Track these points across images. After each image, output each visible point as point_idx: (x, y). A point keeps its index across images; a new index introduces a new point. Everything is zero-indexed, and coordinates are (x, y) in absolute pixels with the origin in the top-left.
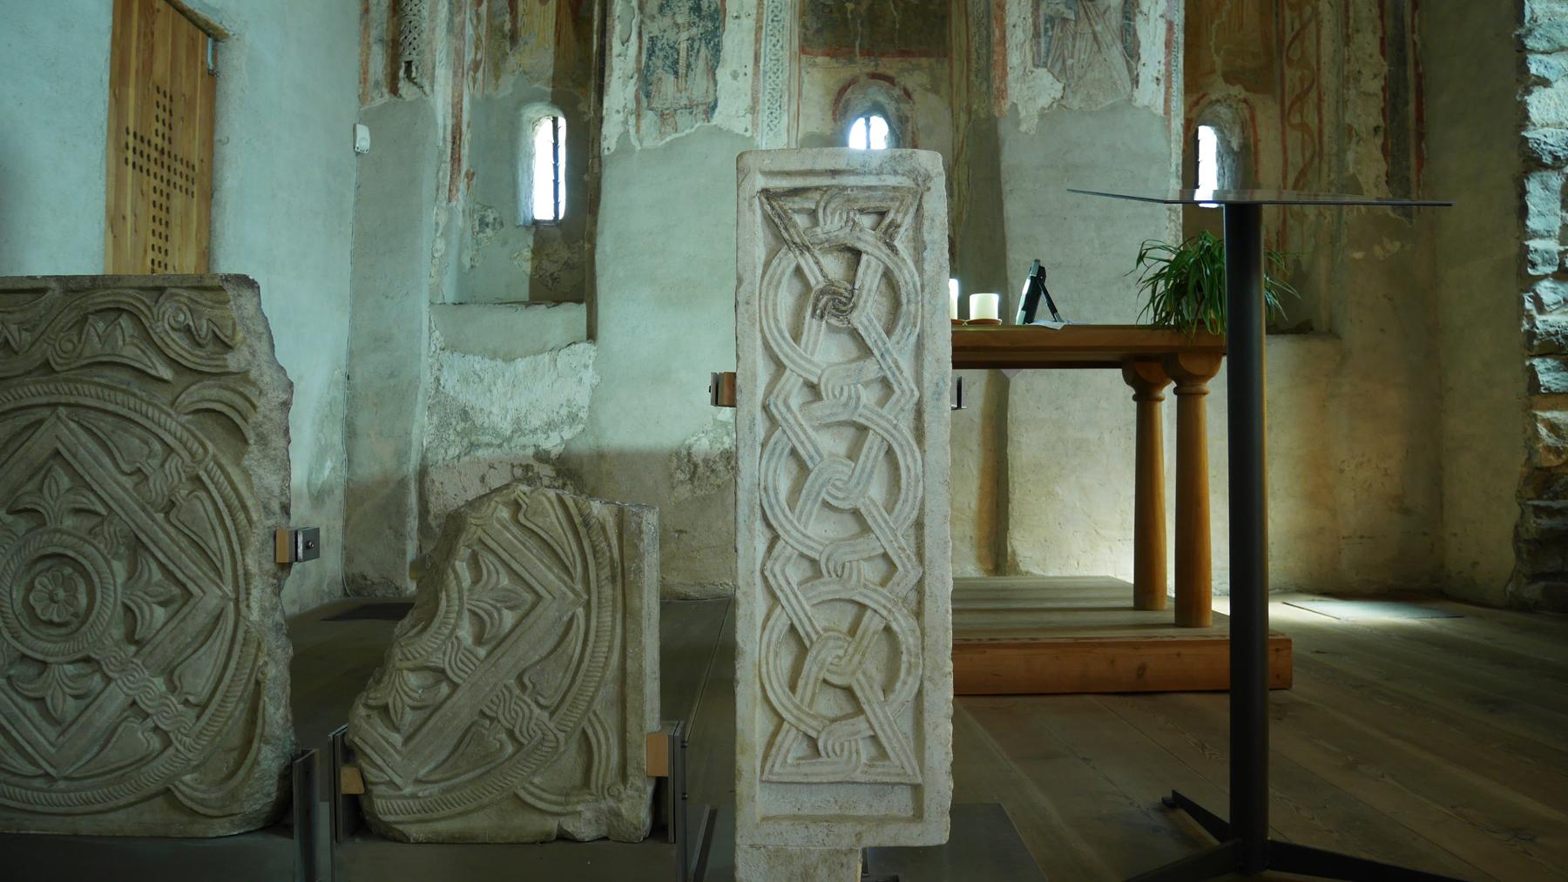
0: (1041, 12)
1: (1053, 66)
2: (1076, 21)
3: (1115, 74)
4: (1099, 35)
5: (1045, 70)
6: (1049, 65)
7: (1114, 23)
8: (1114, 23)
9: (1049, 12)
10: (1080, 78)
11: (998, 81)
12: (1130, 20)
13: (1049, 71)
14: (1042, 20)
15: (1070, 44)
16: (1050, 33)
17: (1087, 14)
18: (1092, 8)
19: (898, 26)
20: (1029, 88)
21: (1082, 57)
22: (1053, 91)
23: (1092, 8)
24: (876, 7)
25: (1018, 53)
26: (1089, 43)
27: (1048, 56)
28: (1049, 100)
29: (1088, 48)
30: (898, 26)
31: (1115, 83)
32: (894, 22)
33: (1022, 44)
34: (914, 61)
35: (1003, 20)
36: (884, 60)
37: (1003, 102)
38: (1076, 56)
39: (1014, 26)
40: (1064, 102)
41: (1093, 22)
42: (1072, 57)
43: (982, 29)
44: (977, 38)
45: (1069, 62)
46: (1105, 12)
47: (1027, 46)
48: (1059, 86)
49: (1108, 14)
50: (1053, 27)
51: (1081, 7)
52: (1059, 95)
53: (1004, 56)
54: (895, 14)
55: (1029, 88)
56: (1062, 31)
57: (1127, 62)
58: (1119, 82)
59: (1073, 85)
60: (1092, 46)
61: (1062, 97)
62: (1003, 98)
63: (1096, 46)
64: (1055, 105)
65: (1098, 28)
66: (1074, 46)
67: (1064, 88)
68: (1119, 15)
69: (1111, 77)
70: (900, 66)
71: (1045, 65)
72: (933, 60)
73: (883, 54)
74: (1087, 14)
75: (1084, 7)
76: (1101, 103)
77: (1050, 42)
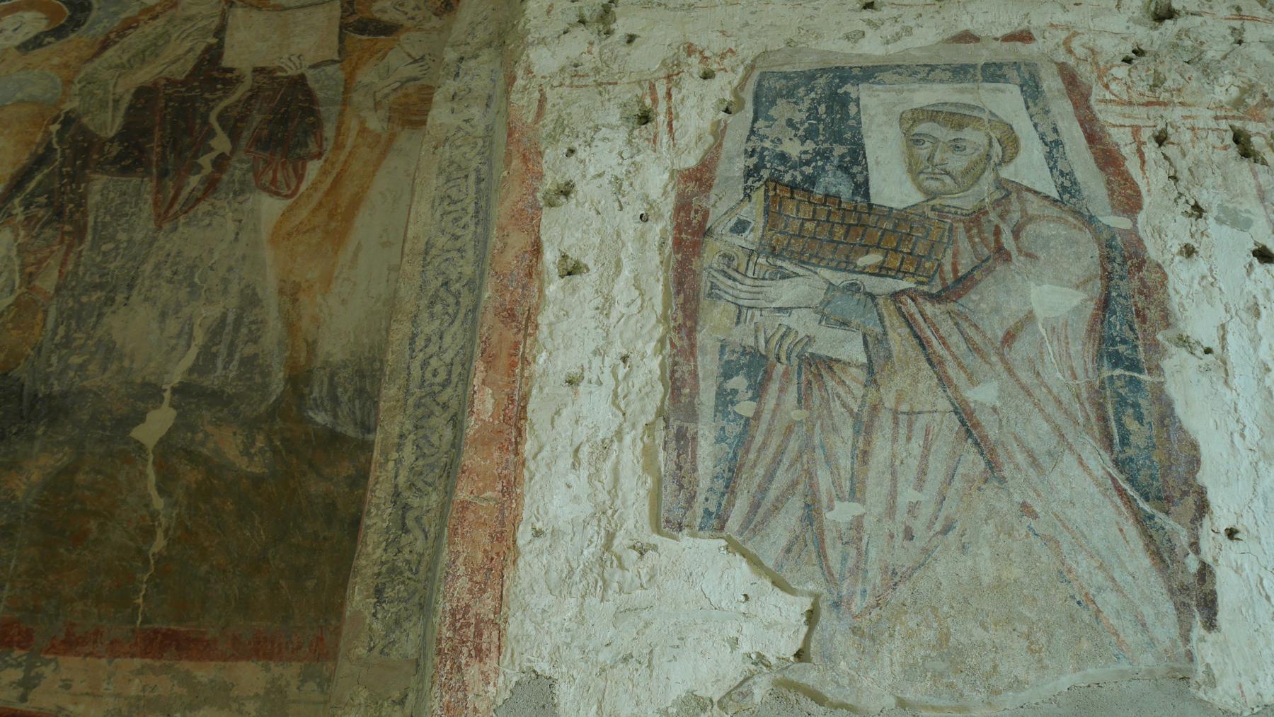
0: (706, 338)
1: (756, 521)
2: (870, 368)
3: (1082, 566)
4: (985, 418)
5: (711, 546)
6: (733, 524)
7: (1055, 376)
8: (1055, 376)
9: (742, 336)
10: (893, 577)
11: (463, 583)
12: (1134, 366)
13: (734, 547)
14: (708, 364)
15: (843, 445)
16: (746, 408)
17: (922, 344)
18: (946, 327)
19: (159, 544)
20: (623, 612)
21: (908, 494)
22: (747, 629)
23: (946, 327)
24: (80, 477)
25: (580, 481)
26: (941, 449)
27: (730, 488)
28: (732, 668)
29: (937, 469)
30: (159, 544)
31: (1087, 601)
32: (149, 533)
33: (606, 447)
34: (204, 672)
35: (518, 360)
36: (72, 665)
37: (473, 672)
38: (876, 491)
39: (572, 382)
40: (810, 676)
41: (952, 370)
42: (856, 492)
43: (439, 421)
44: (408, 452)
45: (840, 514)
46: (1009, 338)
47: (629, 455)
48: (793, 609)
49: (1022, 349)
50: (758, 391)
51: (892, 320)
52: (787, 646)
53: (510, 487)
54: (159, 503)
55: (623, 612)
56: (803, 400)
57: (1143, 522)
58: (1109, 602)
59: (857, 604)
60: (956, 458)
61: (799, 655)
62: (479, 653)
63: (973, 462)
64: (760, 690)
65: (983, 395)
66: (864, 456)
67: (812, 616)
68: (1080, 351)
69: (1064, 575)
70: (134, 688)
71: (716, 522)
72: (289, 672)
73: (70, 644)
74: (922, 344)
75: (909, 322)
76: (1017, 685)
77: (744, 439)
